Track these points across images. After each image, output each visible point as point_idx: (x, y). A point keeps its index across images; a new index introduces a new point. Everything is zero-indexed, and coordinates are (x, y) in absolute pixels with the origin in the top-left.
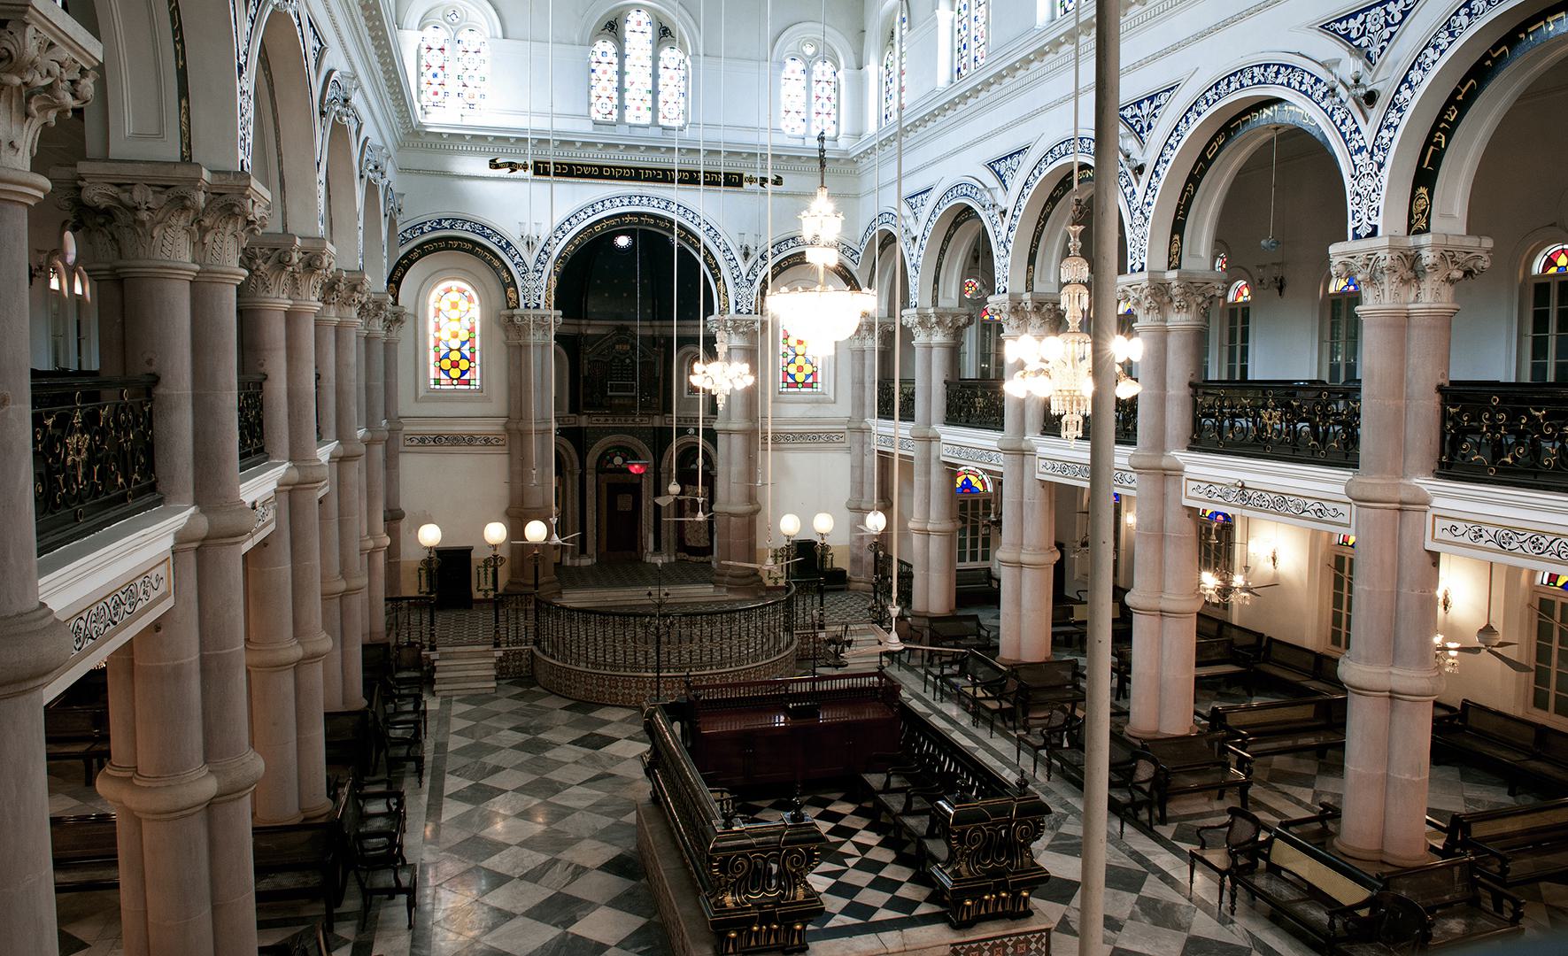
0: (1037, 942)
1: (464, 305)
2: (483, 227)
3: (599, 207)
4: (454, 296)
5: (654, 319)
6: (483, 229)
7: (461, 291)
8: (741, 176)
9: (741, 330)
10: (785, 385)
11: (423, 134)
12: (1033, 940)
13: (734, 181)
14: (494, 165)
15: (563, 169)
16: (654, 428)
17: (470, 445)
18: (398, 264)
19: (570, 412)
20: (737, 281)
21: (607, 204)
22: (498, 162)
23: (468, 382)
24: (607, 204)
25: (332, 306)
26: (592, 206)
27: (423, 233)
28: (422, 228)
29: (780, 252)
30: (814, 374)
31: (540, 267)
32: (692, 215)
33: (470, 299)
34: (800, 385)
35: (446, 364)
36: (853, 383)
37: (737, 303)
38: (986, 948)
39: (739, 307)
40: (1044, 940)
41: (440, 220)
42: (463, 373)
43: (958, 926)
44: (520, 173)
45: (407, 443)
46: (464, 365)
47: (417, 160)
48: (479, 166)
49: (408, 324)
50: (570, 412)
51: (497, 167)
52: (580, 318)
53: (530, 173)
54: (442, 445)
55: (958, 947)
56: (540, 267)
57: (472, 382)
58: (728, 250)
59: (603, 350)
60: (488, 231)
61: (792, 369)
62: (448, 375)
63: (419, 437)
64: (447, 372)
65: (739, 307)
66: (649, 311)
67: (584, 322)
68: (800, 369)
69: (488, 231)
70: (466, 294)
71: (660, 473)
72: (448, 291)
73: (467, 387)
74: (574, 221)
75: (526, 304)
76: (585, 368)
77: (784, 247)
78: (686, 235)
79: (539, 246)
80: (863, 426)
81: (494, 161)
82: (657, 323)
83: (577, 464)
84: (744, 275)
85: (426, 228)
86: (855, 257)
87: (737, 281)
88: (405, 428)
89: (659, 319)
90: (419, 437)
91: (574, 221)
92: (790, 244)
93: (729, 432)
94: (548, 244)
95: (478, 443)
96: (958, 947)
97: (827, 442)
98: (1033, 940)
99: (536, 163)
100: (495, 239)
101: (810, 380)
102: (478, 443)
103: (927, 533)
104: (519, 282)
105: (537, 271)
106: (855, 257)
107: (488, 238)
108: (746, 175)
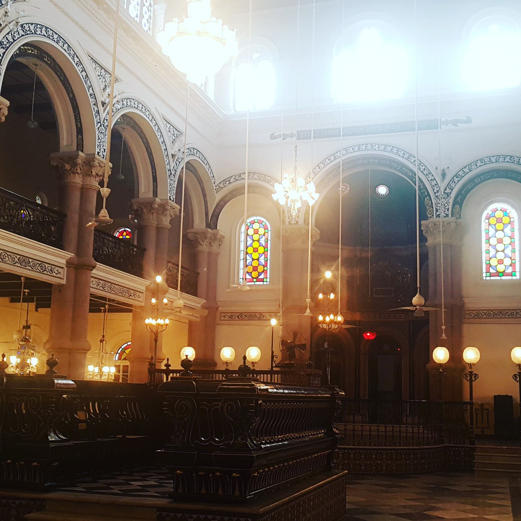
1: (261, 231)
2: (265, 175)
4: (256, 226)
7: (260, 222)
20: (437, 194)
22: (275, 135)
23: (262, 280)
26: (334, 154)
27: (230, 183)
28: (230, 180)
30: (513, 265)
35: (250, 269)
37: (437, 210)
41: (240, 174)
42: (260, 274)
45: (223, 318)
46: (261, 269)
51: (275, 138)
54: (242, 320)
57: (265, 280)
60: (268, 178)
61: (494, 262)
62: (251, 276)
63: (229, 315)
64: (250, 274)
68: (501, 262)
70: (264, 224)
73: (262, 283)
75: (289, 222)
81: (273, 134)
84: (442, 190)
85: (232, 180)
87: (437, 194)
88: (220, 309)
90: (229, 315)
99: (298, 132)
101: (510, 270)
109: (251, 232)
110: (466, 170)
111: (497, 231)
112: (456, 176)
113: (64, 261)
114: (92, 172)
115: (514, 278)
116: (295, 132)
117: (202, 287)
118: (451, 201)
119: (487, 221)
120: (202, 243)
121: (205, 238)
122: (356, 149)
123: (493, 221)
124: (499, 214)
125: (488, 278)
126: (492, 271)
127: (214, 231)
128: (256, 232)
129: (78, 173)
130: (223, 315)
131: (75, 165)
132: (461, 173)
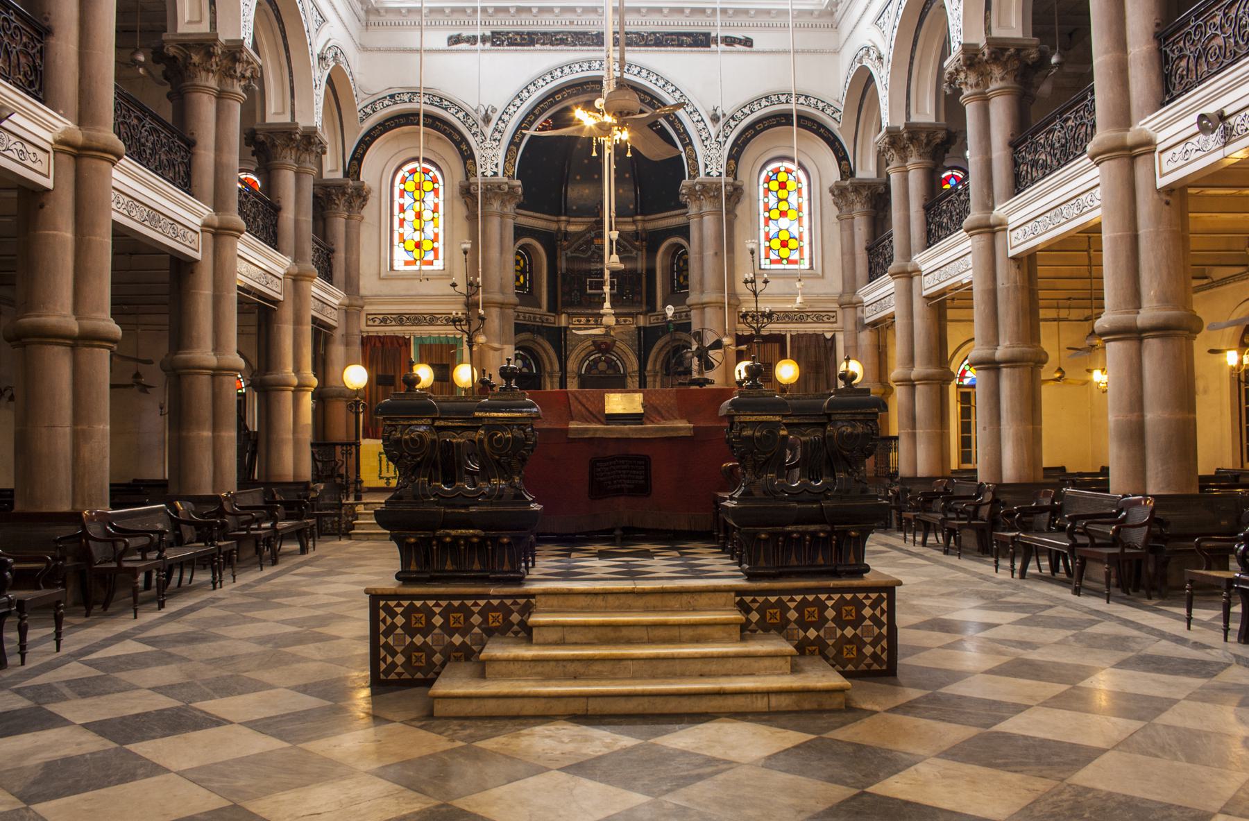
0: (873, 607)
2: (441, 99)
3: (558, 73)
5: (637, 214)
6: (440, 101)
8: (707, 35)
9: (712, 194)
10: (768, 261)
11: (382, 11)
12: (867, 602)
13: (701, 41)
14: (455, 40)
15: (523, 39)
16: (639, 328)
17: (430, 325)
18: (362, 141)
19: (549, 311)
21: (567, 70)
23: (431, 263)
24: (567, 70)
25: (211, 75)
29: (752, 112)
31: (497, 135)
32: (655, 77)
33: (434, 180)
34: (785, 261)
36: (843, 254)
37: (706, 166)
38: (792, 605)
39: (708, 170)
40: (884, 605)
43: (751, 577)
44: (479, 45)
45: (370, 323)
47: (379, 38)
48: (438, 39)
49: (372, 202)
50: (549, 311)
52: (559, 214)
53: (488, 45)
55: (748, 599)
56: (497, 135)
58: (696, 111)
59: (581, 246)
63: (381, 317)
65: (708, 170)
66: (631, 207)
67: (563, 218)
69: (446, 103)
71: (645, 377)
72: (413, 172)
74: (532, 88)
76: (563, 265)
77: (756, 107)
78: (651, 101)
79: (495, 117)
80: (854, 300)
82: (639, 218)
83: (557, 367)
86: (836, 115)
89: (642, 214)
90: (381, 317)
91: (532, 88)
92: (764, 103)
93: (703, 306)
94: (505, 112)
95: (439, 323)
96: (748, 599)
97: (815, 322)
98: (867, 602)
100: (453, 111)
102: (439, 323)
103: (910, 384)
104: (477, 154)
105: (495, 140)
106: (836, 115)
107: (446, 109)
108: (713, 34)
109: (410, 186)
110: (747, 111)
111: (780, 200)
112: (732, 118)
113: (199, 222)
114: (235, 72)
115: (802, 267)
116: (488, 33)
117: (339, 273)
118: (725, 154)
119: (766, 185)
120: (337, 202)
121: (344, 193)
122: (586, 66)
123: (774, 185)
124: (782, 177)
125: (767, 267)
126: (773, 256)
127: (356, 183)
128: (419, 187)
129: (213, 71)
130: (371, 317)
131: (210, 55)
132: (739, 114)
